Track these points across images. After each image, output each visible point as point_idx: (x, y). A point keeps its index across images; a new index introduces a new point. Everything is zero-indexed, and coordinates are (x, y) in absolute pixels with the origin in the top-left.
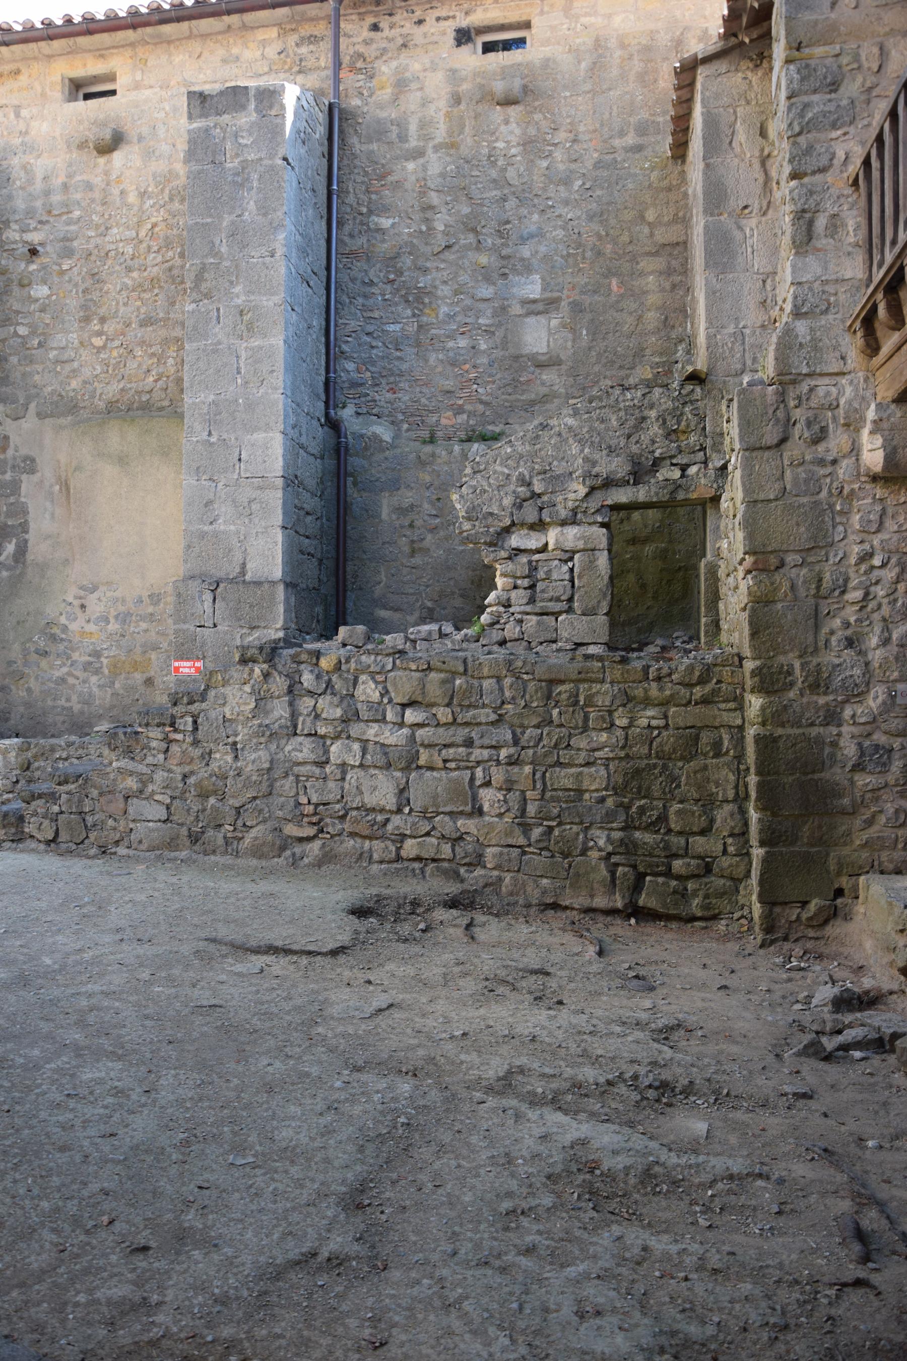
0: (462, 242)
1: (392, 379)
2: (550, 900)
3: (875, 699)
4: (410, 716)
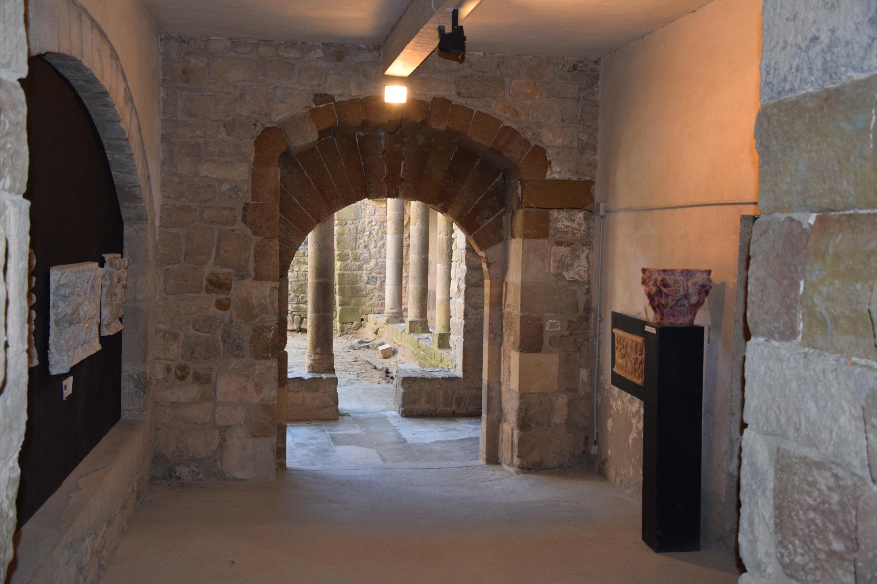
3: (372, 263)
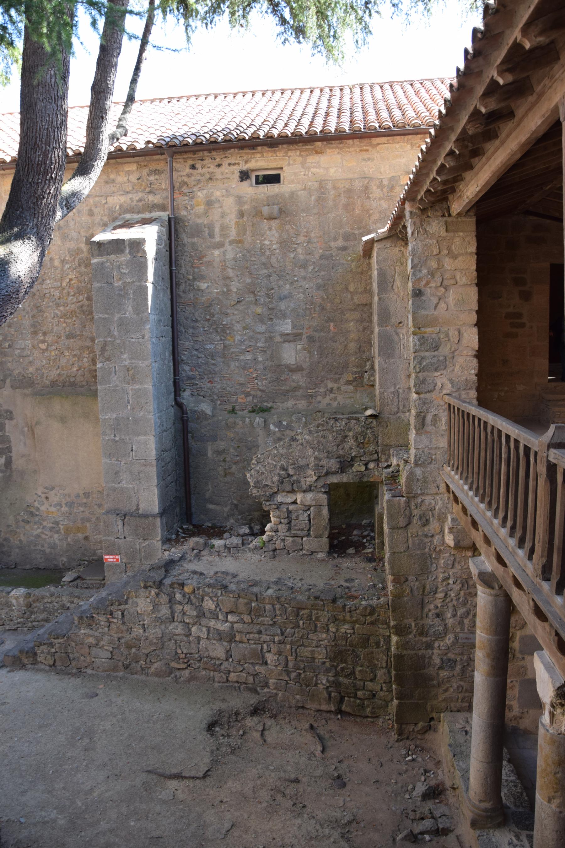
0: (247, 299)
1: (210, 376)
2: (300, 705)
3: (449, 639)
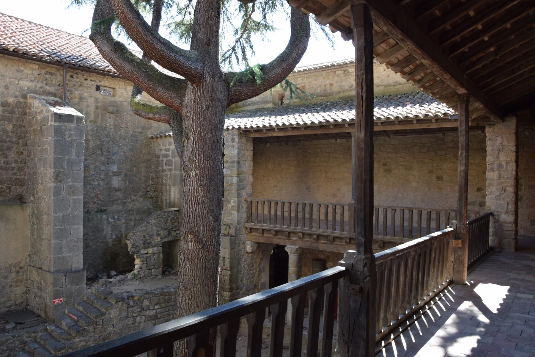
4: (156, 307)
